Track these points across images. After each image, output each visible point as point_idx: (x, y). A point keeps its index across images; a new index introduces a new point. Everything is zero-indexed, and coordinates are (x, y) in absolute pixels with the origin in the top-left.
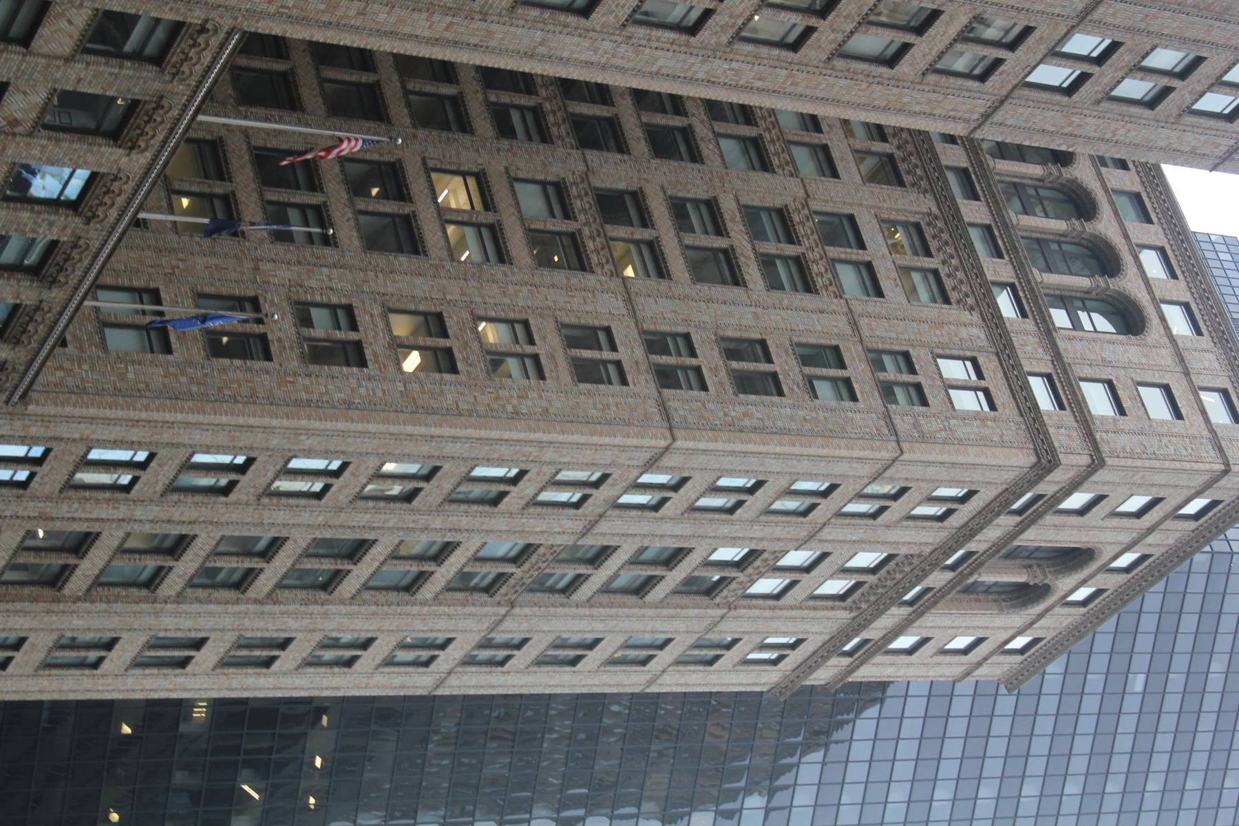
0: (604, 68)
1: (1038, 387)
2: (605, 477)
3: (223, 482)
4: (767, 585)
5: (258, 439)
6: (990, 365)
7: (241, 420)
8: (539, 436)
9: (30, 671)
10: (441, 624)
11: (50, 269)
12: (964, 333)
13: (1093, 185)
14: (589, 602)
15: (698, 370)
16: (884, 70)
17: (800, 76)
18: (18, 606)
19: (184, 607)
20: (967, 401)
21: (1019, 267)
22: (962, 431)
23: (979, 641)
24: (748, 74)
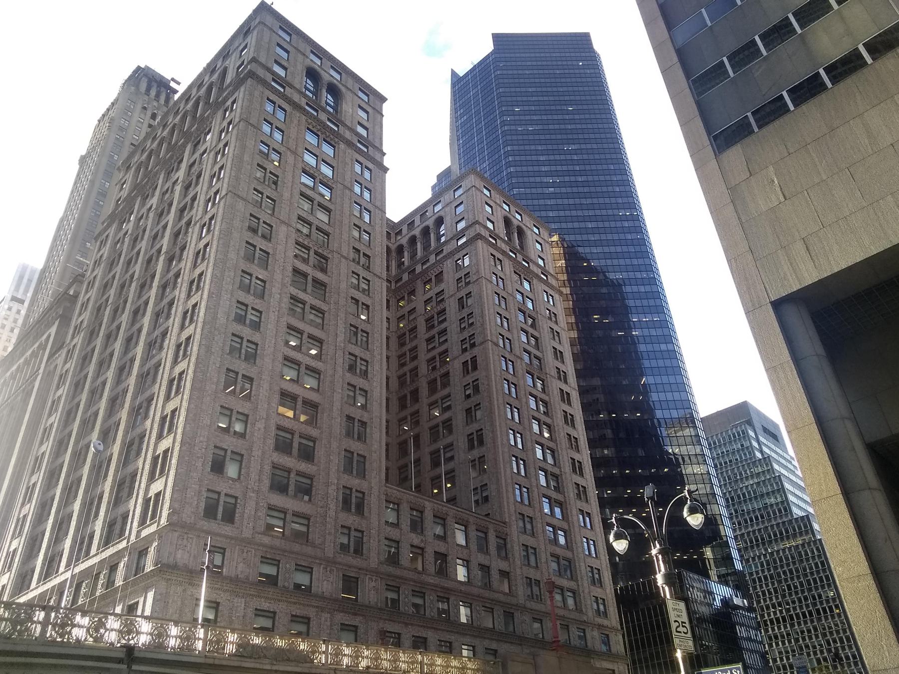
0: (381, 383)
1: (460, 243)
2: (502, 356)
3: (522, 462)
4: (530, 305)
5: (506, 455)
6: (457, 257)
7: (501, 460)
8: (493, 377)
9: (589, 506)
10: (555, 392)
11: (464, 523)
12: (449, 265)
13: (407, 237)
14: (542, 352)
15: (470, 337)
16: (371, 308)
17: (376, 330)
18: (569, 513)
19: (562, 466)
20: (467, 262)
21: (431, 254)
22: (474, 261)
23: (537, 241)
24: (377, 344)
